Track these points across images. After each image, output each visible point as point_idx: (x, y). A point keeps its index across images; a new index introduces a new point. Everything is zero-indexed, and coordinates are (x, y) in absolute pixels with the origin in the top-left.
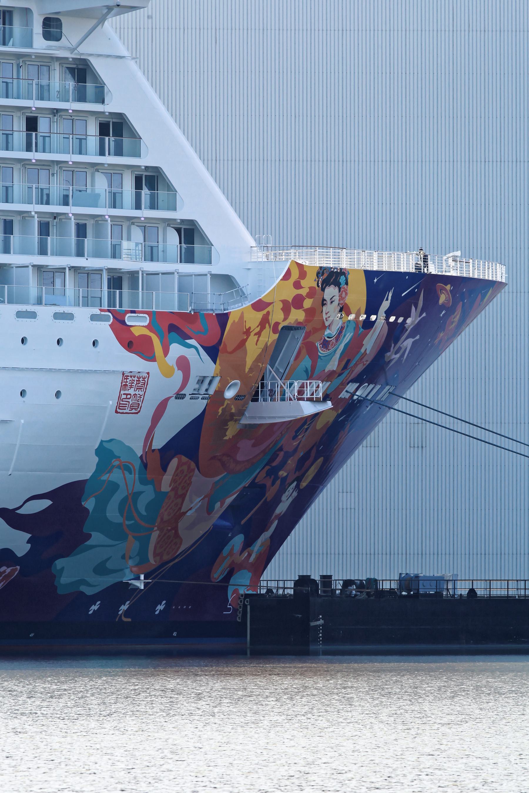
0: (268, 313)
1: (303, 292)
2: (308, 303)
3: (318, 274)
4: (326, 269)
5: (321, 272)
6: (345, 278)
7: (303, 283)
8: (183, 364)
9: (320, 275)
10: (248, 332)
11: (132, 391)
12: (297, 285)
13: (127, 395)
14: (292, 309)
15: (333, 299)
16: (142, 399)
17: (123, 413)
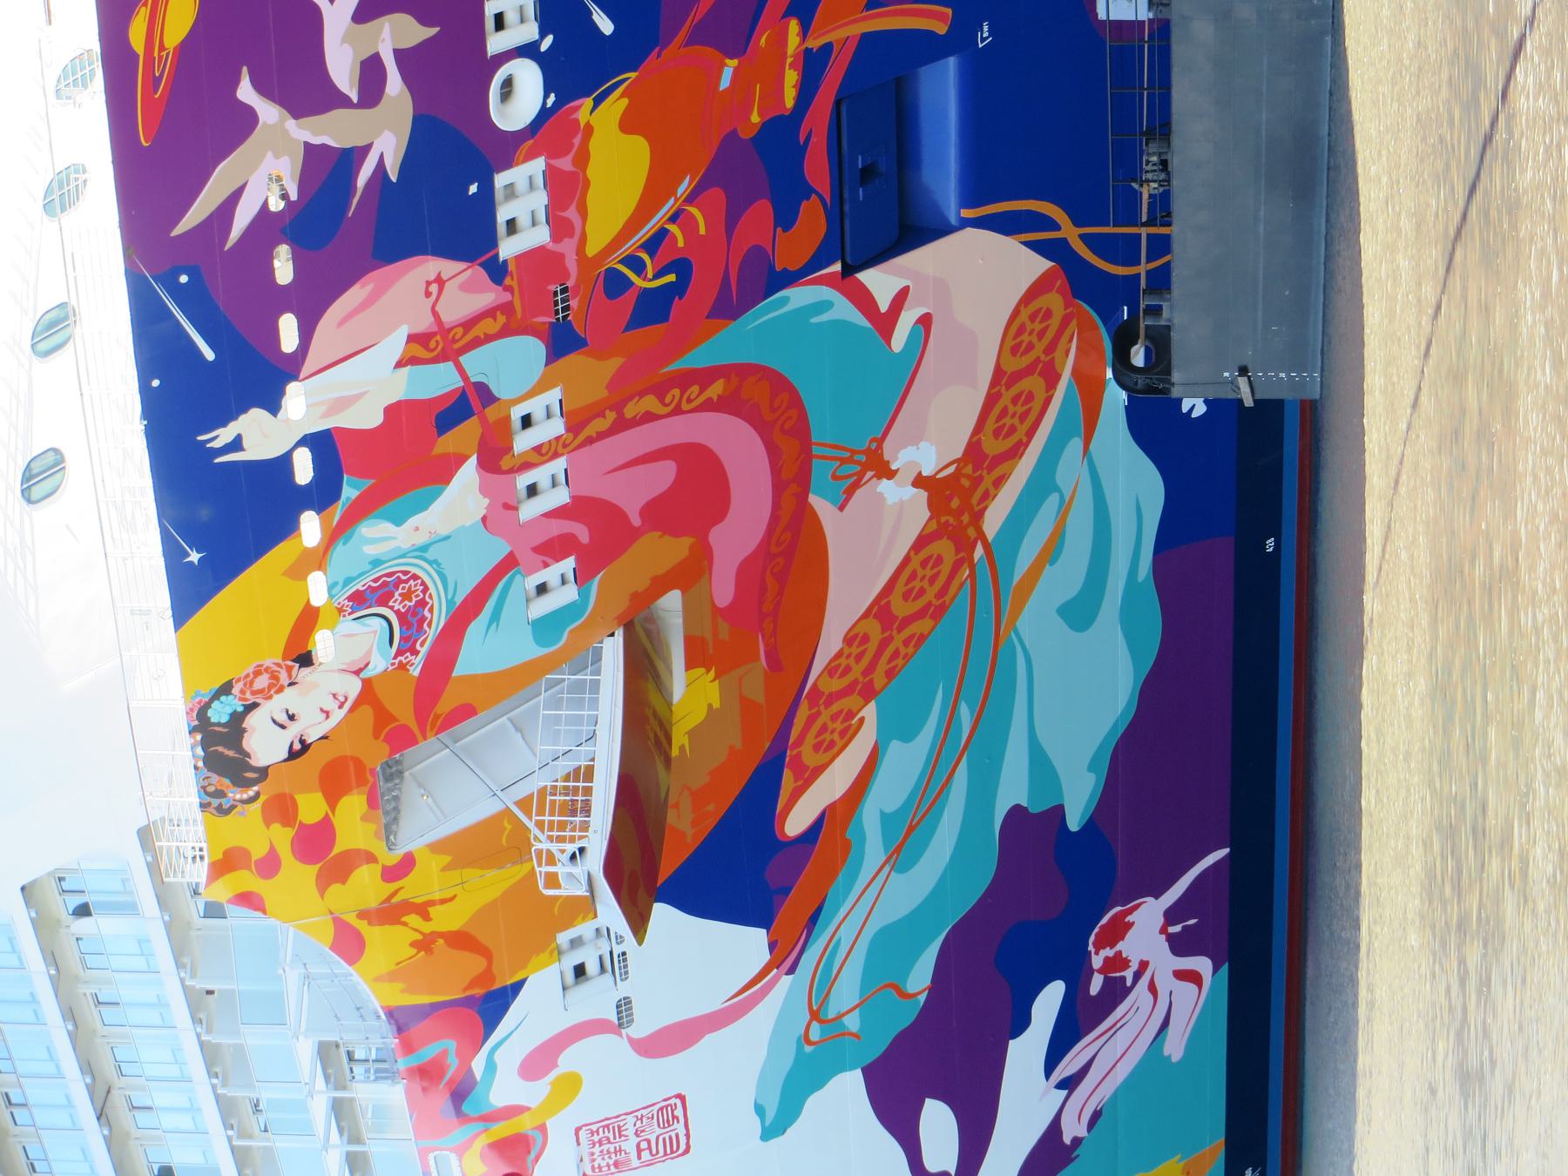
0: (363, 915)
1: (282, 837)
2: (311, 807)
3: (223, 811)
4: (204, 788)
5: (215, 802)
6: (215, 704)
7: (258, 852)
8: (538, 1063)
9: (223, 801)
10: (424, 944)
11: (629, 1146)
12: (269, 866)
13: (639, 1151)
14: (337, 850)
15: (282, 718)
16: (644, 1112)
17: (688, 1136)
